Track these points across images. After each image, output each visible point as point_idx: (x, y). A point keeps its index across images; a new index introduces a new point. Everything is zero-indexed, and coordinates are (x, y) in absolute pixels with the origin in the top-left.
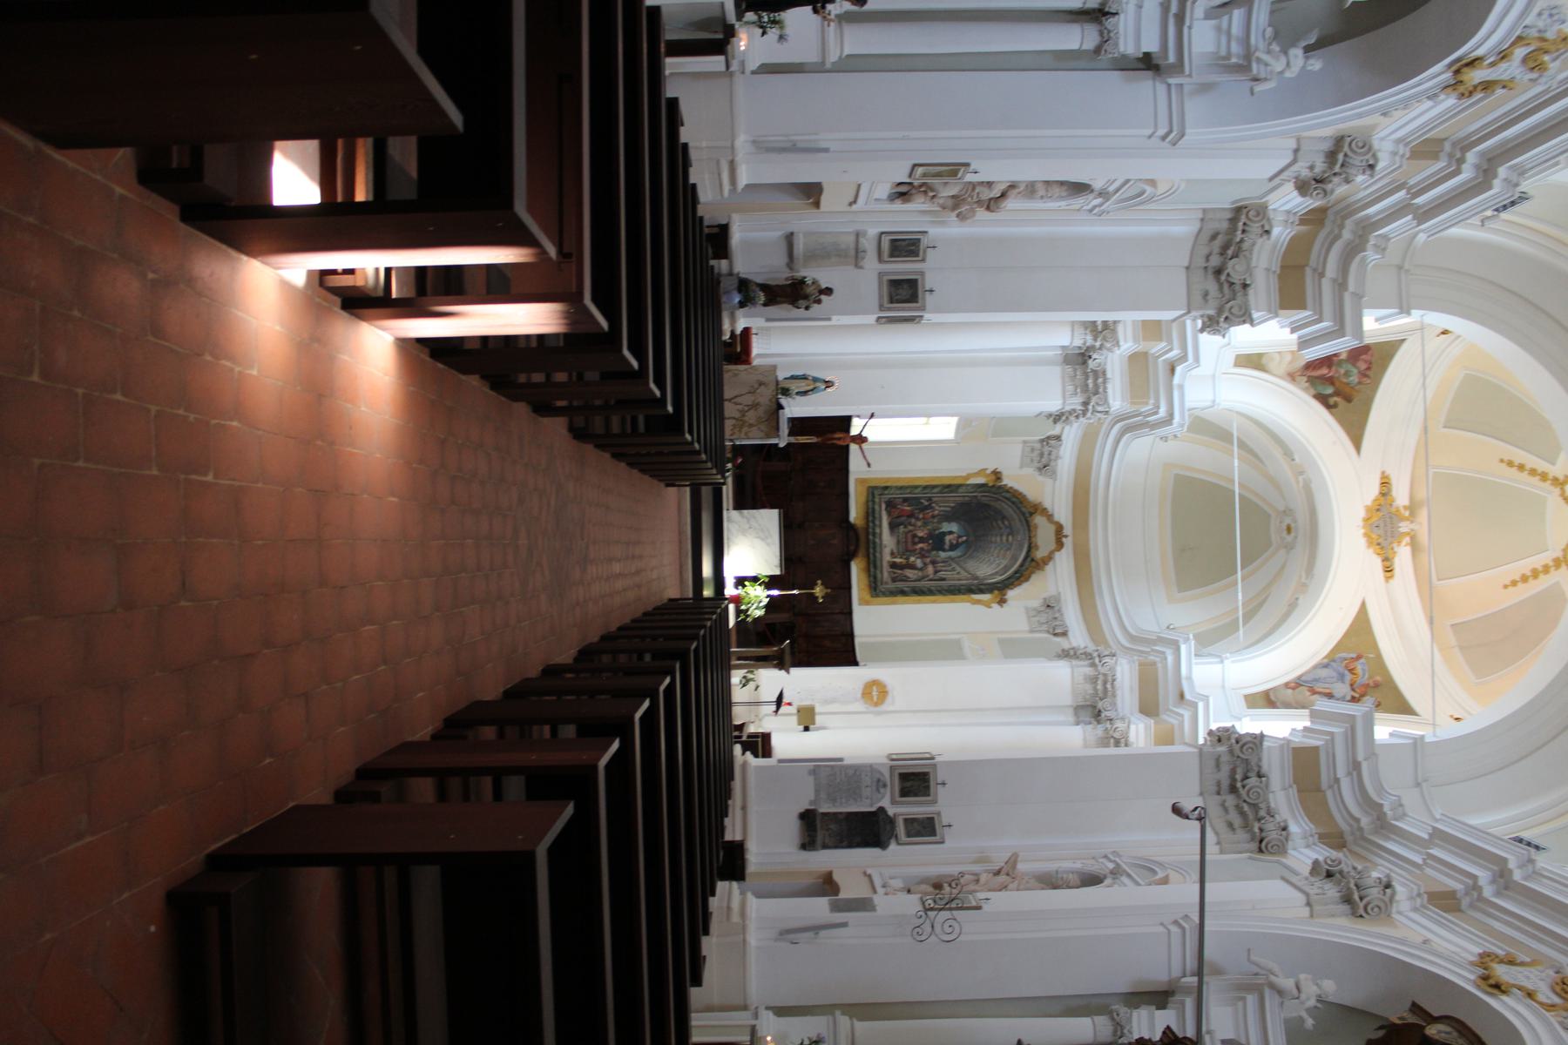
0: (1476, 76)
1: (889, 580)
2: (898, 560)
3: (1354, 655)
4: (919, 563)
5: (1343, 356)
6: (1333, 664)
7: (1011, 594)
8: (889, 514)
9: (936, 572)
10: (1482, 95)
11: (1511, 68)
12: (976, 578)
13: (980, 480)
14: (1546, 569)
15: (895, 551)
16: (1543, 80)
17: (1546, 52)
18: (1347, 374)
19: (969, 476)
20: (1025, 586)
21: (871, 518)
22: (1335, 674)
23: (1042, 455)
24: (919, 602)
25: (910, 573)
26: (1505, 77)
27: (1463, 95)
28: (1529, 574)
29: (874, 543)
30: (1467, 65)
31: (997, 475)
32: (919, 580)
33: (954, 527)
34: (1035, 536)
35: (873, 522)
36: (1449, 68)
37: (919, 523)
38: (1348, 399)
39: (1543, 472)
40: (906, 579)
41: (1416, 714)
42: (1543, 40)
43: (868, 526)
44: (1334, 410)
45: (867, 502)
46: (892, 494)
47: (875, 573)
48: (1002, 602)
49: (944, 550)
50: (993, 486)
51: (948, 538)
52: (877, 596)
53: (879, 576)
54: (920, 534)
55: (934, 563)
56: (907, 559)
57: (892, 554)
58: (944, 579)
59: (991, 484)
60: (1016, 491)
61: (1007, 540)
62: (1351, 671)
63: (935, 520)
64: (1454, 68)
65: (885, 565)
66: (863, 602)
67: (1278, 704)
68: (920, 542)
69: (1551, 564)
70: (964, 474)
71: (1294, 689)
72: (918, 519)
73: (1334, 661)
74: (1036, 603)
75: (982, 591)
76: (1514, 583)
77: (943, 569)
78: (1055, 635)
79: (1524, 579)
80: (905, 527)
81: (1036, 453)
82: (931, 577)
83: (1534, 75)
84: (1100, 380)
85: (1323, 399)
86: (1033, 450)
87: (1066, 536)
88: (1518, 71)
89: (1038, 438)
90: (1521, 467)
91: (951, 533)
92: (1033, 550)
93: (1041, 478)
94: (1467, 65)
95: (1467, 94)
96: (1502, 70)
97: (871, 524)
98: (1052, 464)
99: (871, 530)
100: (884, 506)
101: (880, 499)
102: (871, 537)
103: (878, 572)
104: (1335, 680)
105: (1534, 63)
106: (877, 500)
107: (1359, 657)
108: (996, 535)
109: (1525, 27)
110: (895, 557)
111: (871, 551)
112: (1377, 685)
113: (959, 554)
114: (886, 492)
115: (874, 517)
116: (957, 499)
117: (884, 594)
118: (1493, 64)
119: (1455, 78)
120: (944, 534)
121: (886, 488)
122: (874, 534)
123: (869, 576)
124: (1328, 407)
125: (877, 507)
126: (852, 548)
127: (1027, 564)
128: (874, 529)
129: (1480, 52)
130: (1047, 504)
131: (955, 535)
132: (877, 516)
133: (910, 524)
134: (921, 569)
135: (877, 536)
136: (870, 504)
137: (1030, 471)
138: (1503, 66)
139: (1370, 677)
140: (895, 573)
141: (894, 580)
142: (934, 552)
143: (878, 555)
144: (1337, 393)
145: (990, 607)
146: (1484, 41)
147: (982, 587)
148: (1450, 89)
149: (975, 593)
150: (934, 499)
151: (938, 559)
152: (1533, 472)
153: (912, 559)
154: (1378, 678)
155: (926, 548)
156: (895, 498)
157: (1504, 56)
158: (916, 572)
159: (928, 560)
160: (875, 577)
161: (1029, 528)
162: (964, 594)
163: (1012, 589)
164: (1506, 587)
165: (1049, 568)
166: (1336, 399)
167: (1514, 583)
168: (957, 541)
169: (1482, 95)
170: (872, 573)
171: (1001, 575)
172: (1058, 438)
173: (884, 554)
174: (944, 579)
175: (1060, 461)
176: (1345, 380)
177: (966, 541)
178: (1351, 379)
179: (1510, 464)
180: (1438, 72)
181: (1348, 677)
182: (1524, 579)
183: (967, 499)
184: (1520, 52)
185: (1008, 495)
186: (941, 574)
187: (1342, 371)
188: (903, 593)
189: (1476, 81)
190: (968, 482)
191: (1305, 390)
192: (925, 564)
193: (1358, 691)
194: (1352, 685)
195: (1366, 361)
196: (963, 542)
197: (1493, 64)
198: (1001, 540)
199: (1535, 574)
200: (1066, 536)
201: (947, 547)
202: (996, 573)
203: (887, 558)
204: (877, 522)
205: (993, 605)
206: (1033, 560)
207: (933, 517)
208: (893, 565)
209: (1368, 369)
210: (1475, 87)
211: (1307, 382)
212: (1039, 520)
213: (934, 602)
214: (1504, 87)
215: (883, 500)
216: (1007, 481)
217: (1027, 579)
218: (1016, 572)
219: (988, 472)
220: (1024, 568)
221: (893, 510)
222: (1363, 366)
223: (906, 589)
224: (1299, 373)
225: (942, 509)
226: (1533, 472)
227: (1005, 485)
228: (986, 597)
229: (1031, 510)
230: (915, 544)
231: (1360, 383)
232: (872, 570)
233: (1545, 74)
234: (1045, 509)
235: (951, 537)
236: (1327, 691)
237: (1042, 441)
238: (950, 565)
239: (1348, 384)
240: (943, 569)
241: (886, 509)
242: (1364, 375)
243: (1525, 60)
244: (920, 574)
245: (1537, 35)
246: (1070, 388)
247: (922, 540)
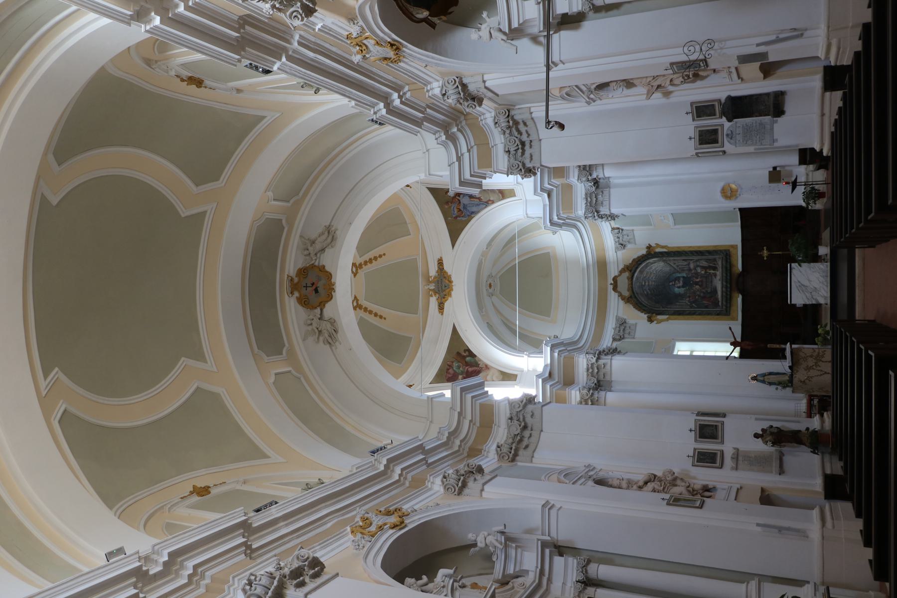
0: (393, 519)
2: (712, 271)
3: (458, 218)
4: (699, 270)
5: (460, 377)
6: (469, 214)
7: (644, 252)
8: (717, 299)
9: (689, 264)
10: (391, 508)
11: (377, 521)
12: (664, 261)
13: (660, 317)
14: (366, 263)
15: (714, 277)
16: (363, 512)
17: (361, 527)
18: (459, 367)
19: (667, 320)
20: (635, 256)
21: (729, 297)
22: (468, 208)
23: (624, 330)
24: (699, 247)
25: (705, 264)
26: (380, 517)
27: (399, 510)
28: (373, 261)
29: (726, 282)
30: (397, 526)
31: (650, 320)
32: (699, 260)
33: (677, 290)
34: (629, 285)
35: (727, 294)
36: (406, 525)
37: (698, 293)
38: (458, 354)
39: (366, 312)
40: (707, 260)
41: (428, 188)
42: (362, 533)
44: (467, 348)
45: (730, 307)
48: (649, 247)
49: (684, 277)
50: (653, 313)
51: (681, 284)
52: (725, 250)
53: (724, 263)
54: (697, 287)
55: (690, 270)
56: (706, 272)
57: (715, 275)
58: (684, 260)
59: (654, 315)
60: (639, 310)
61: (645, 283)
62: (460, 210)
63: (688, 295)
64: (403, 525)
65: (720, 270)
66: (735, 247)
67: (497, 191)
68: (698, 282)
69: (363, 266)
70: (670, 321)
71: (489, 200)
72: (699, 296)
73: (468, 215)
74: (629, 246)
75: (661, 253)
76: (380, 256)
77: (684, 266)
78: (618, 228)
79: (376, 258)
80: (707, 291)
81: (627, 332)
82: (691, 262)
83: (366, 515)
84: (590, 370)
85: (472, 355)
86: (629, 334)
87: (611, 284)
88: (374, 519)
89: (626, 340)
90: (376, 315)
91: (679, 287)
92: (630, 277)
93: (625, 317)
94: (397, 526)
95: (397, 510)
96: (381, 521)
98: (618, 325)
99: (729, 290)
100: (720, 303)
102: (729, 286)
104: (468, 206)
105: (367, 523)
106: (724, 307)
107: (456, 218)
108: (651, 285)
109: (370, 541)
110: (713, 273)
111: (729, 278)
112: (447, 203)
113: (674, 275)
114: (718, 312)
115: (727, 298)
116: (675, 307)
117: (721, 251)
118: (385, 524)
119: (403, 519)
120: (683, 287)
122: (726, 287)
123: (730, 263)
124: (469, 350)
125: (724, 303)
127: (634, 269)
128: (726, 290)
129: (391, 531)
130: (622, 303)
131: (676, 286)
133: (704, 293)
134: (698, 266)
136: (728, 305)
137: (631, 321)
138: (380, 523)
139: (450, 207)
140: (714, 264)
141: (715, 260)
142: (689, 276)
143: (725, 275)
144: (464, 357)
145: (656, 244)
146: (389, 537)
147: (660, 256)
148: (406, 513)
149: (665, 252)
150: (688, 307)
151: (687, 272)
152: (370, 312)
153: (703, 272)
154: (446, 207)
155: (694, 278)
156: (714, 308)
157: (380, 528)
158: (701, 265)
159: (693, 272)
160: (726, 261)
161: (631, 288)
162: (672, 252)
163: (643, 255)
164: (384, 254)
165: (621, 267)
166: (465, 355)
167: (380, 256)
168: (675, 282)
169: (391, 508)
171: (649, 262)
172: (614, 340)
174: (684, 260)
175: (614, 326)
176: (460, 364)
177: (670, 282)
178: (456, 365)
179: (381, 317)
180: (412, 523)
181: (461, 207)
182: (376, 258)
183: (669, 307)
184: (373, 528)
185: (644, 308)
186: (685, 263)
187: (461, 369)
188: (709, 252)
189: (393, 516)
190: (668, 316)
191: (480, 360)
192: (695, 269)
193: (457, 200)
194: (460, 203)
195: (449, 373)
196: (672, 282)
197: (385, 524)
198: (649, 282)
199: (371, 261)
200: (611, 284)
201: (682, 279)
202: (652, 264)
203: (719, 273)
204: (724, 294)
205: (655, 245)
206: (631, 271)
207: (689, 297)
208: (715, 268)
209: (448, 369)
210: (393, 513)
211: (479, 364)
212: (626, 294)
213: (691, 247)
214: (380, 511)
216: (645, 316)
217: (634, 260)
218: (641, 264)
219: (655, 322)
220: (635, 267)
222: (451, 371)
223: (707, 254)
224: (483, 369)
225: (684, 301)
226: (370, 312)
227: (645, 314)
228: (658, 250)
229: (630, 299)
230: (702, 281)
231: (453, 362)
232: (728, 266)
233: (362, 515)
234: (622, 300)
235: (679, 285)
236: (472, 199)
237: (623, 338)
238: (680, 268)
239: (459, 362)
240: (684, 266)
241: (719, 302)
242: (451, 366)
243: (371, 524)
244: (698, 263)
245: (365, 536)
246: (608, 367)
247: (697, 283)
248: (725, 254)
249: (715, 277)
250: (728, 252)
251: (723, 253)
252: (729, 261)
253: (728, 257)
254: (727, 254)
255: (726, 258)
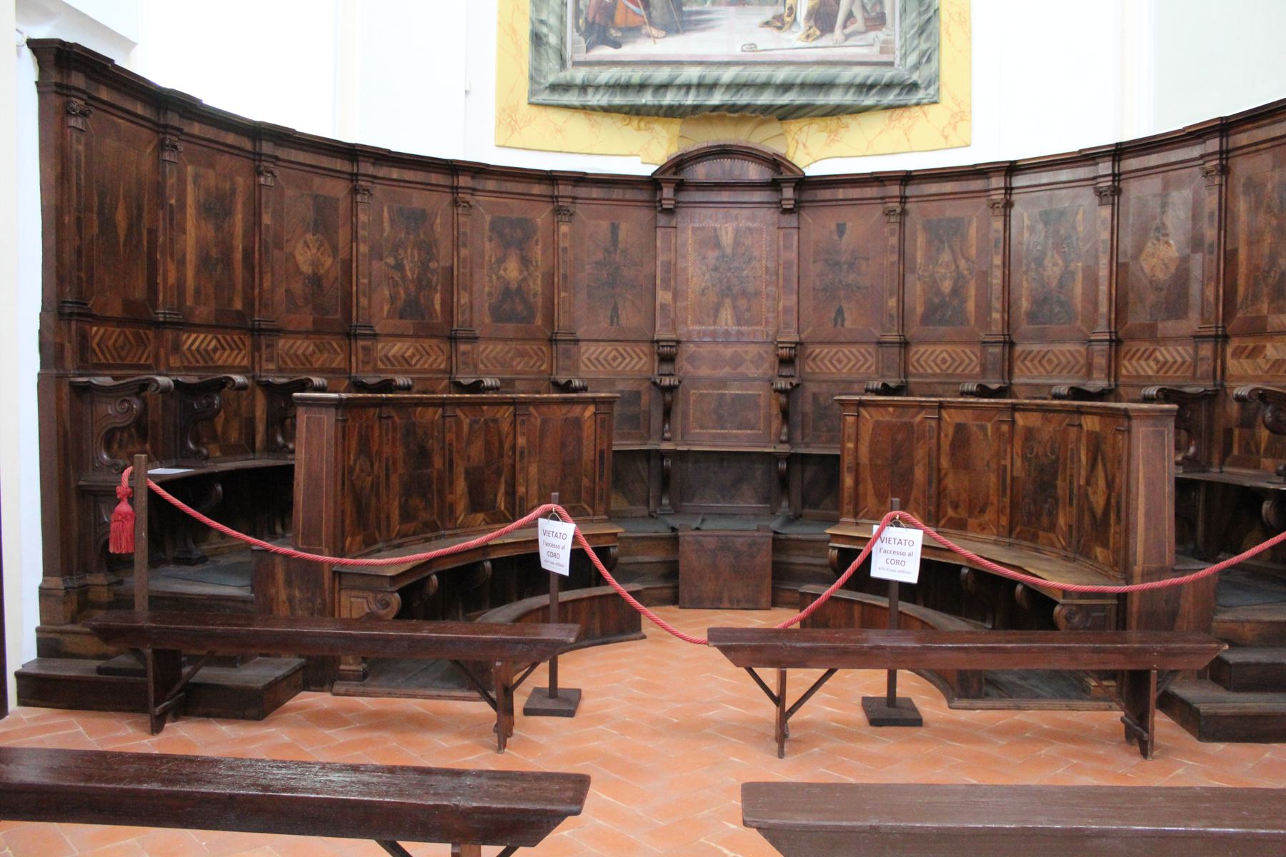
1: (881, 35)
8: (633, 31)
15: (768, 13)
21: (647, 99)
35: (663, 87)
43: (671, 112)
45: (584, 108)
46: (562, 19)
47: (848, 86)
52: (933, 80)
53: (860, 74)
57: (778, 23)
97: (669, 99)
99: (691, 100)
100: (605, 52)
101: (577, 64)
102: (717, 99)
103: (847, 75)
106: (579, 75)
111: (765, 99)
114: (553, 40)
115: (642, 87)
117: (927, 57)
121: (537, 39)
125: (605, 75)
126: (754, 172)
128: (688, 87)
132: (636, 75)
135: (711, 74)
140: (850, 16)
141: (877, 21)
143: (781, 75)
156: (577, 13)
160: (865, 87)
170: (849, 99)
173: (777, 56)
204: (662, 75)
215: (581, 57)
221: (619, 18)
232: (835, 98)
241: (617, 45)
248: (915, 77)
249: (767, 24)
250: (921, 94)
251: (916, 67)
252: (870, 101)
253: (891, 98)
254: (914, 87)
255: (889, 86)
